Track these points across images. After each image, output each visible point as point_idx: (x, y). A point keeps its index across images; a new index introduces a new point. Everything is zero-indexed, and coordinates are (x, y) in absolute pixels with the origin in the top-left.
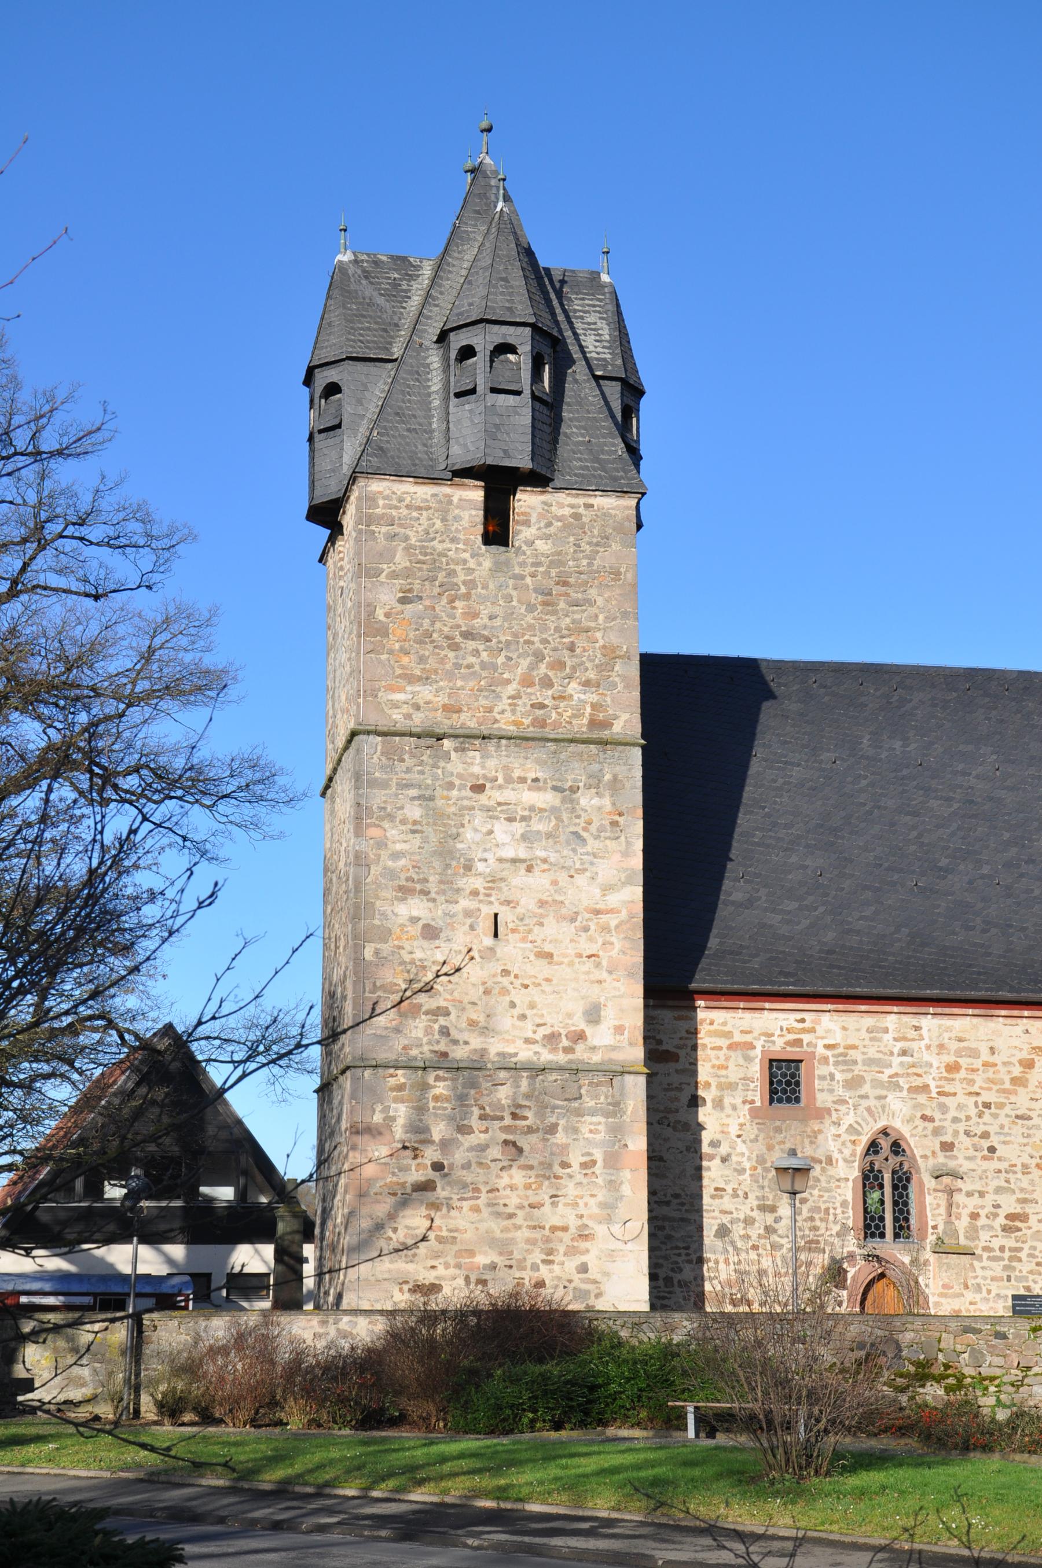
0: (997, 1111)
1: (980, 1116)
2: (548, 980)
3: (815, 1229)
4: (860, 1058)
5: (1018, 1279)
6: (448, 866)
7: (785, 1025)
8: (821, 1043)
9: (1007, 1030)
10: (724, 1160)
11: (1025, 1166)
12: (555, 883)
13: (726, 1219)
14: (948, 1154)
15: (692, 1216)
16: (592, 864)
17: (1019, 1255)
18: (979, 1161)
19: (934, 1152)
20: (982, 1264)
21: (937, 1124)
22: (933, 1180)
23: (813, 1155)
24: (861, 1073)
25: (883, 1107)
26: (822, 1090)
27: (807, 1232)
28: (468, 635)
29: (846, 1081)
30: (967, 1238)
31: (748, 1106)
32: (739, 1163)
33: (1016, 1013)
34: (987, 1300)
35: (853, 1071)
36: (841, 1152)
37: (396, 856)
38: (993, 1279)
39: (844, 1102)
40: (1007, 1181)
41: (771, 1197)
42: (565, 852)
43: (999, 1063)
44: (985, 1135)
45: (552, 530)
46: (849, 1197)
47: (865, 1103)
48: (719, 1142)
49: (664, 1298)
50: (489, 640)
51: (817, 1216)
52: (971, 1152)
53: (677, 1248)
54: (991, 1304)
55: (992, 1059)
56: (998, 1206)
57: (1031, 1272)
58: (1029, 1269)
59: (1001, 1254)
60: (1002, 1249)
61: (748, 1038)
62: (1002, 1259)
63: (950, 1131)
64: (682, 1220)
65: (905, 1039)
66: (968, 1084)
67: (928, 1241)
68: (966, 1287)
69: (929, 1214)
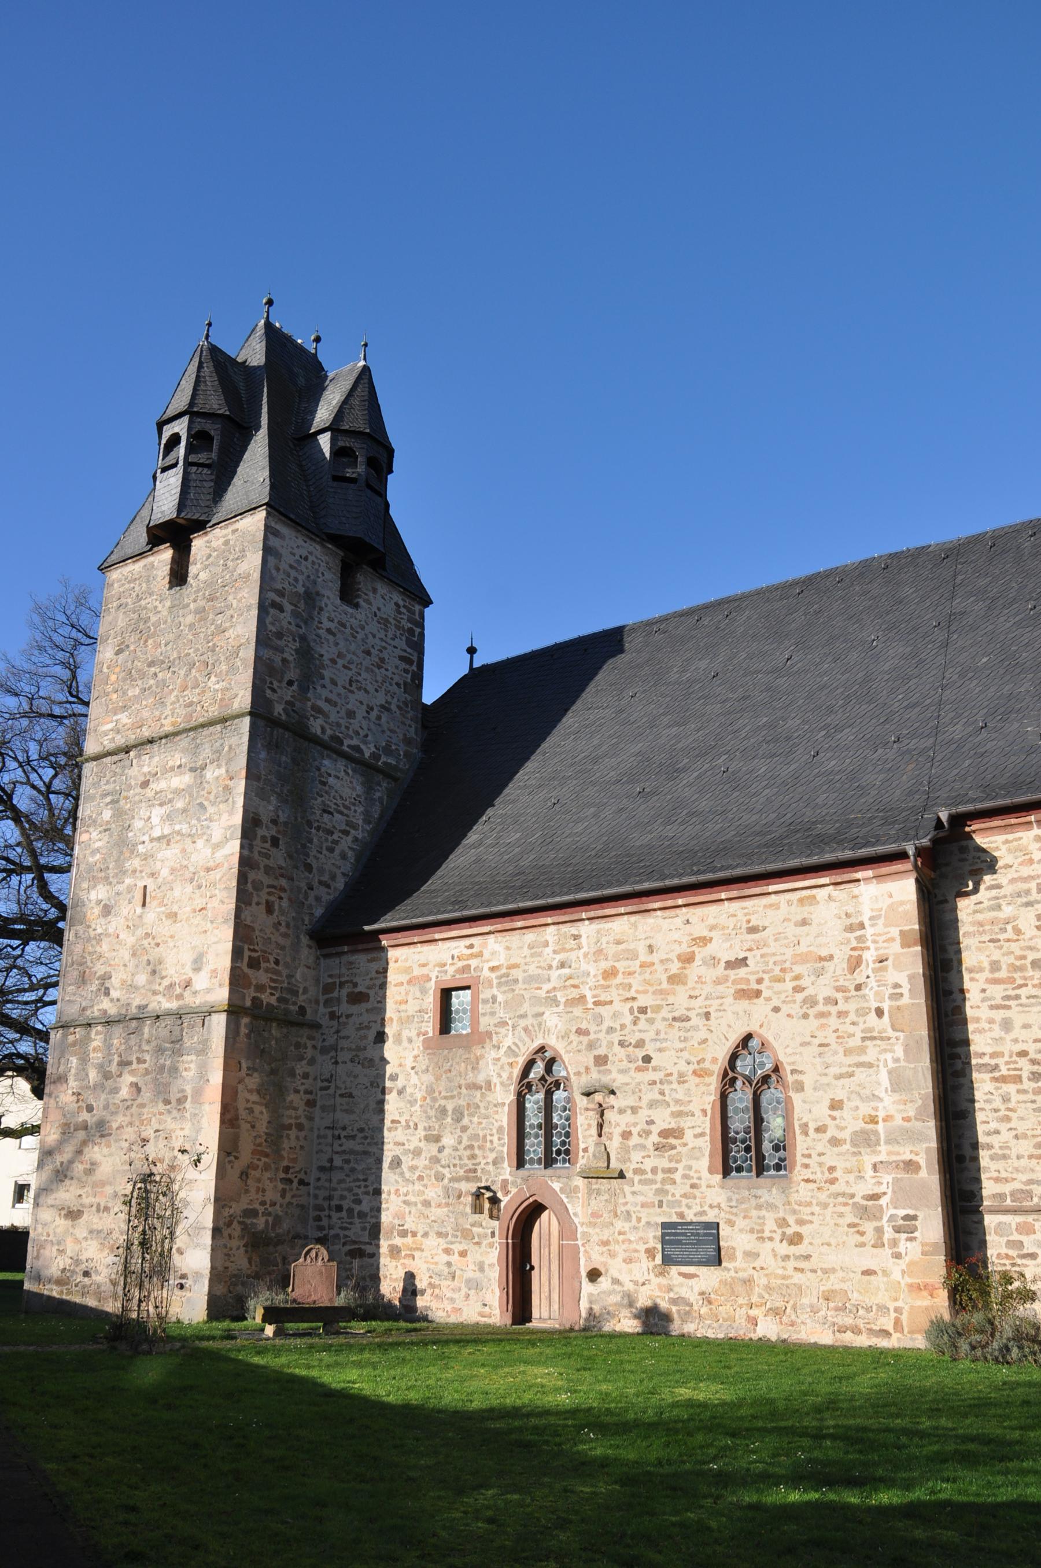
0: (654, 1015)
1: (635, 1023)
2: (172, 937)
3: (473, 1157)
5: (671, 1204)
6: (121, 853)
7: (456, 953)
9: (665, 924)
10: (400, 1092)
11: (681, 1075)
12: (184, 851)
13: (398, 1151)
14: (602, 1068)
15: (373, 1149)
16: (208, 827)
17: (672, 1176)
18: (632, 1073)
19: (587, 1069)
20: (634, 1189)
21: (592, 1036)
22: (585, 1098)
24: (522, 992)
25: (540, 1025)
26: (484, 1014)
28: (151, 664)
29: (506, 1002)
30: (618, 1159)
31: (422, 1038)
32: (412, 1095)
33: (670, 903)
34: (635, 1228)
35: (513, 990)
36: (499, 1075)
37: (94, 852)
38: (643, 1206)
40: (662, 1093)
41: (437, 1127)
42: (194, 822)
43: (656, 961)
44: (640, 1044)
45: (211, 560)
46: (505, 1124)
47: (523, 1023)
48: (397, 1075)
49: (346, 1229)
50: (163, 662)
51: (476, 1144)
52: (625, 1064)
53: (358, 1180)
55: (649, 959)
56: (651, 1122)
57: (685, 1196)
58: (682, 1192)
59: (654, 1177)
60: (654, 1171)
61: (424, 971)
62: (653, 1182)
63: (604, 1043)
64: (365, 1153)
65: (564, 950)
66: (624, 989)
68: (616, 1215)
69: (580, 1136)
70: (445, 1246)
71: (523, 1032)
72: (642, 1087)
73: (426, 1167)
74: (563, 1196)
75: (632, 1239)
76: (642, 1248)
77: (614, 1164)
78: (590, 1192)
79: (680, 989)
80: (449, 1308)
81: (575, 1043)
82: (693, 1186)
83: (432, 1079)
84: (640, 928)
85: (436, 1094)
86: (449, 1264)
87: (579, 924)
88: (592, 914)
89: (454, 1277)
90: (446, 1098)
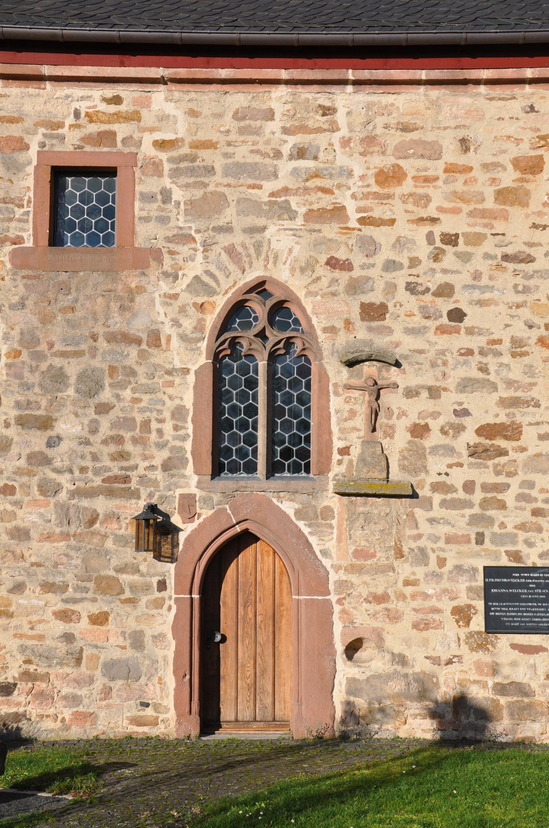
0: (469, 249)
1: (436, 257)
3: (123, 456)
4: (219, 163)
5: (497, 539)
7: (83, 106)
8: (148, 139)
11: (517, 342)
14: (375, 324)
17: (500, 496)
18: (431, 336)
19: (348, 323)
20: (431, 514)
21: (357, 273)
22: (345, 370)
23: (125, 329)
24: (221, 189)
25: (258, 246)
26: (146, 220)
27: (108, 463)
29: (191, 203)
30: (403, 468)
34: (437, 576)
35: (205, 185)
36: (176, 323)
38: (449, 540)
39: (189, 239)
40: (484, 369)
41: (44, 403)
43: (476, 166)
47: (224, 240)
51: (127, 435)
52: (417, 320)
54: (445, 584)
55: (462, 160)
56: (466, 413)
57: (522, 527)
58: (518, 521)
59: (468, 497)
60: (469, 487)
62: (468, 504)
65: (303, 129)
66: (416, 204)
67: (331, 475)
68: (400, 554)
69: (335, 428)
70: (61, 606)
71: (224, 257)
72: (448, 357)
73: (19, 472)
74: (301, 524)
75: (430, 592)
76: (447, 605)
77: (395, 474)
78: (352, 518)
79: (515, 212)
80: (67, 713)
81: (325, 282)
82: (536, 513)
83: (35, 321)
84: (446, 109)
85: (43, 347)
86: (69, 638)
87: (334, 89)
88: (366, 74)
89: (78, 661)
90: (63, 354)
